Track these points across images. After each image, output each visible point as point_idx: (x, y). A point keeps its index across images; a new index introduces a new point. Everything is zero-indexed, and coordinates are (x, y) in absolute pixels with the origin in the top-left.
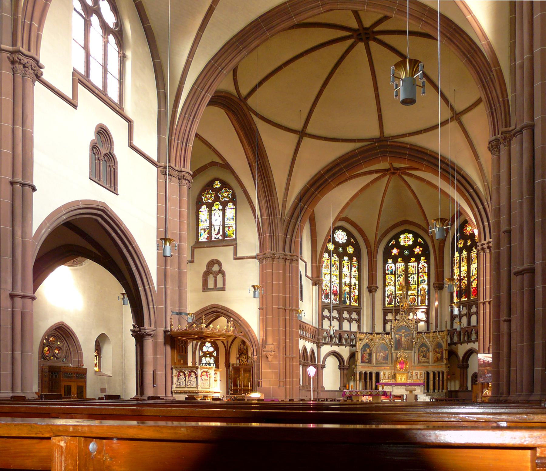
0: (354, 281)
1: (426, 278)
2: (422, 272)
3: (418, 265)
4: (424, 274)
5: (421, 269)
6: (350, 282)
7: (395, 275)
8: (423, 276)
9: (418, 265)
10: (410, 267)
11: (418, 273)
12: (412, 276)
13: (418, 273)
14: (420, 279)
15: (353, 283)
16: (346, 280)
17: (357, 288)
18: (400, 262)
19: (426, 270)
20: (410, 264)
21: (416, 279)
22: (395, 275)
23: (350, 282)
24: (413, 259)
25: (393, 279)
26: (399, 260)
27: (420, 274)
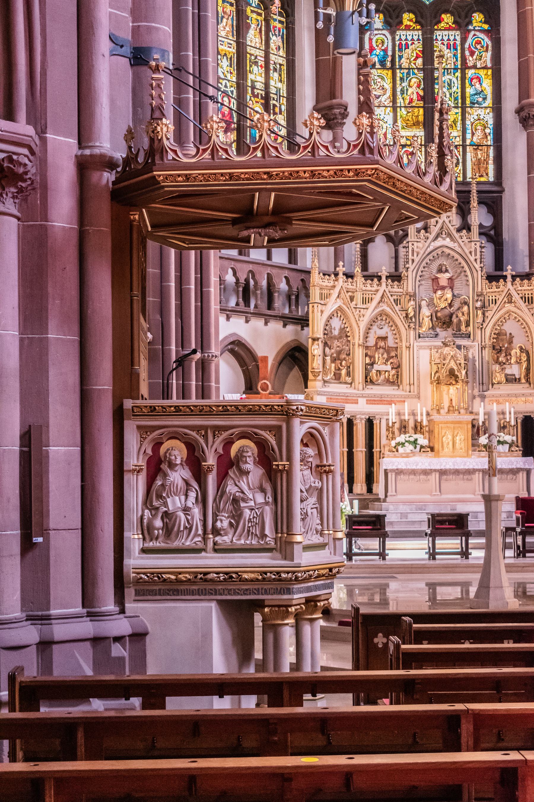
0: (278, 84)
1: (487, 85)
2: (474, 67)
3: (464, 40)
4: (482, 73)
5: (472, 53)
6: (267, 85)
7: (393, 68)
8: (479, 79)
9: (464, 40)
10: (438, 46)
11: (465, 67)
12: (446, 78)
13: (465, 67)
14: (469, 91)
15: (273, 90)
16: (256, 75)
17: (283, 108)
18: (408, 28)
19: (488, 56)
20: (438, 34)
21: (456, 88)
22: (393, 68)
23: (267, 85)
24: (448, 19)
25: (388, 86)
26: (407, 18)
27: (470, 73)
